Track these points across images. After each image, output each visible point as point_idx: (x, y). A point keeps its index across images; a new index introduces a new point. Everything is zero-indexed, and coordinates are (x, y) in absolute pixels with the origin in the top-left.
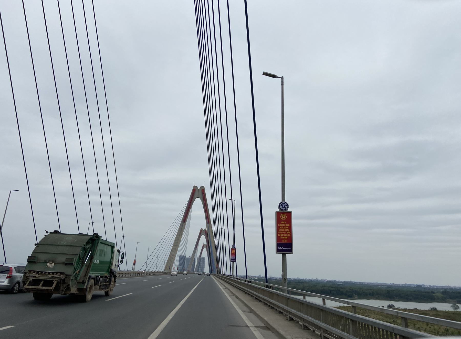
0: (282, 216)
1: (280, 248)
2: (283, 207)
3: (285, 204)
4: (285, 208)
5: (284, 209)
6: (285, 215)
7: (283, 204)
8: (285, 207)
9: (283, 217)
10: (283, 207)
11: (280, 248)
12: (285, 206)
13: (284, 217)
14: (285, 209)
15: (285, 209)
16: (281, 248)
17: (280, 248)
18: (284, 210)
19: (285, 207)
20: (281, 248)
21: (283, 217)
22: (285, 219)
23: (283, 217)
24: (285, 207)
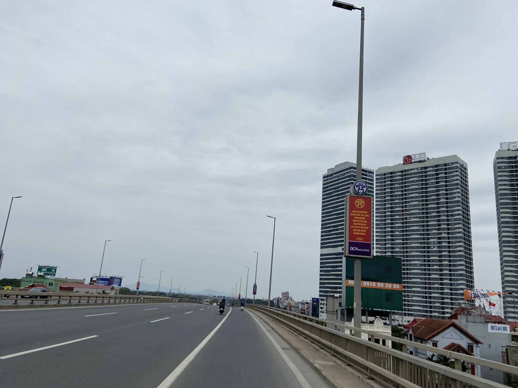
0: (358, 202)
1: (352, 249)
2: (359, 189)
3: (362, 184)
4: (363, 190)
5: (361, 191)
6: (362, 201)
7: (359, 184)
8: (362, 189)
9: (360, 203)
10: (359, 189)
11: (353, 249)
12: (362, 187)
13: (361, 204)
14: (363, 191)
15: (363, 191)
16: (355, 249)
17: (352, 249)
18: (361, 193)
19: (363, 188)
20: (355, 249)
21: (360, 203)
22: (362, 207)
23: (359, 204)
24: (363, 188)
